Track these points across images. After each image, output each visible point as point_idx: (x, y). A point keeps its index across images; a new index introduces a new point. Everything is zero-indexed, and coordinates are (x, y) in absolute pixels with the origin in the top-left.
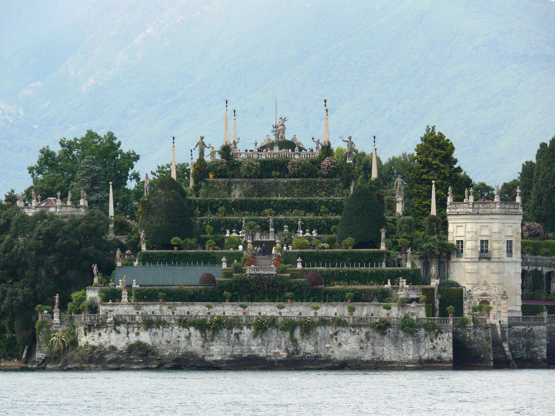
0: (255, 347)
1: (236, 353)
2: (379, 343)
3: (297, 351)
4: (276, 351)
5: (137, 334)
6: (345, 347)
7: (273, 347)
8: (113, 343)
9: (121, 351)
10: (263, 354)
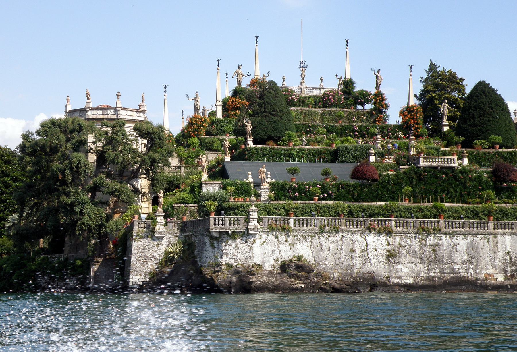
0: (459, 266)
1: (433, 274)
4: (490, 271)
5: (292, 245)
7: (484, 267)
8: (257, 260)
10: (471, 274)
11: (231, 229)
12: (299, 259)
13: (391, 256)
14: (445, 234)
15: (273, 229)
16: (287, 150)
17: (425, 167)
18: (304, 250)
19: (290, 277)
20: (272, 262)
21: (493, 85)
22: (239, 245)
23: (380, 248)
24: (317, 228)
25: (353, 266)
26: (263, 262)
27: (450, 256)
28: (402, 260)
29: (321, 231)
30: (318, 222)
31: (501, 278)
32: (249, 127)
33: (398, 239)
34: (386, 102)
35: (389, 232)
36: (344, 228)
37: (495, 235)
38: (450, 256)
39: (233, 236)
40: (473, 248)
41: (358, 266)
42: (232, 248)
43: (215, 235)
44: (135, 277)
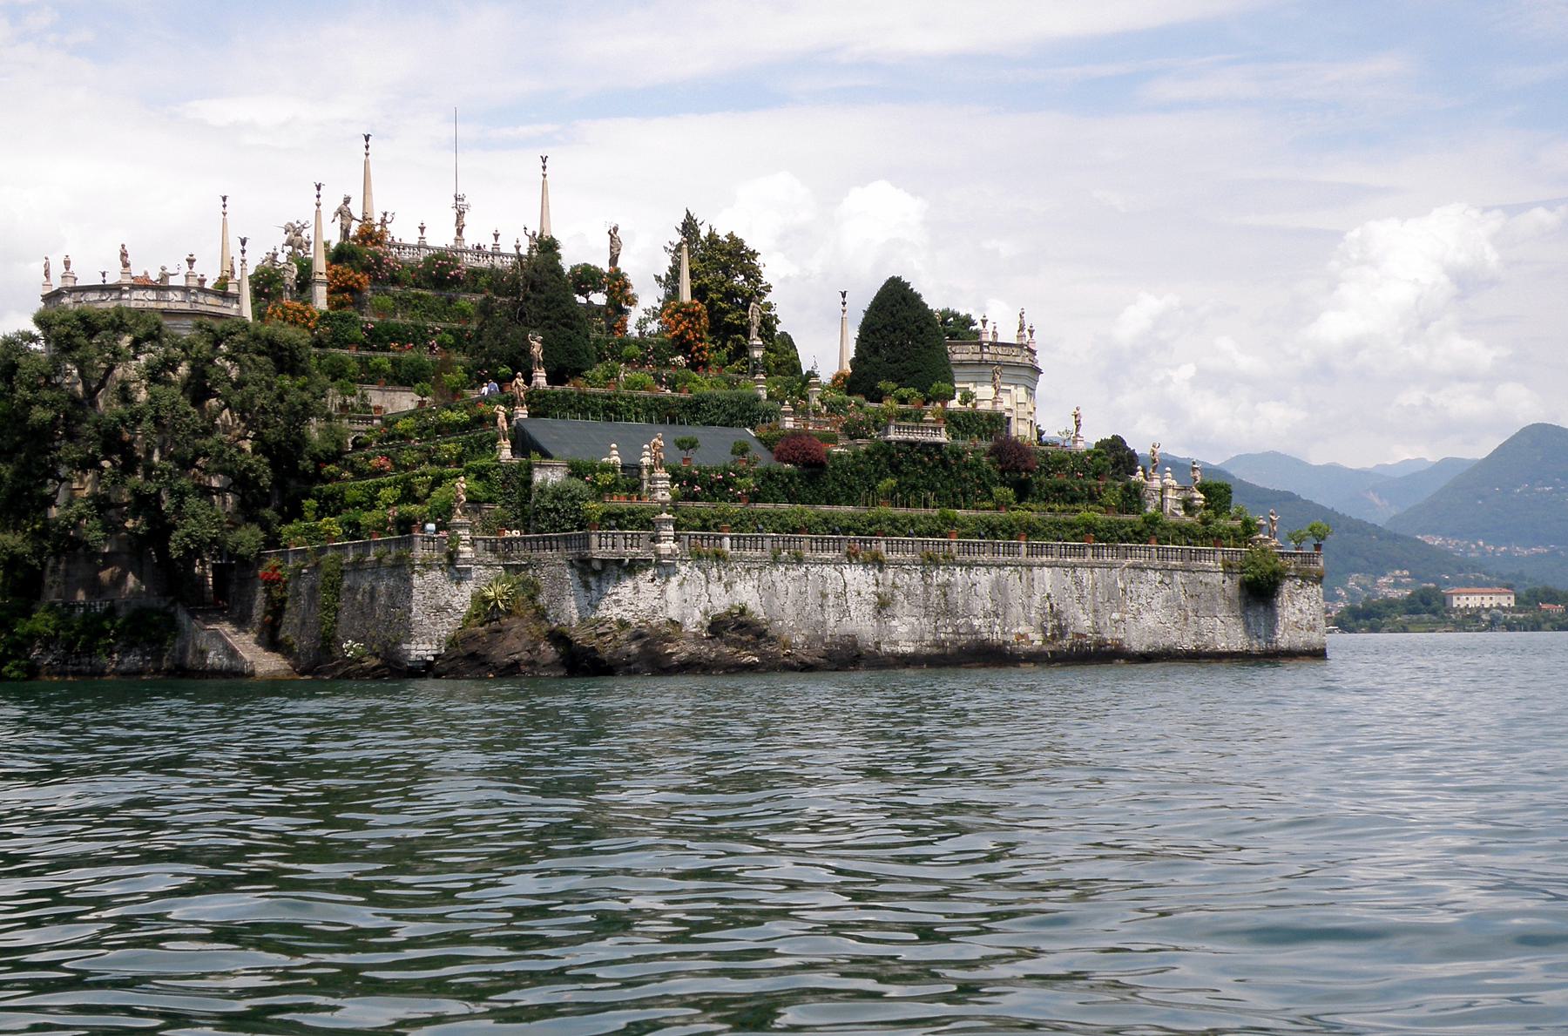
2: (1207, 609)
3: (1061, 631)
4: (1022, 630)
5: (729, 586)
6: (1149, 620)
8: (674, 613)
9: (695, 634)
10: (997, 636)
11: (629, 553)
12: (743, 611)
13: (883, 605)
14: (961, 565)
15: (700, 557)
16: (609, 398)
17: (898, 442)
18: (747, 593)
19: (727, 644)
20: (698, 616)
21: (916, 287)
22: (641, 583)
23: (864, 589)
24: (767, 553)
25: (824, 622)
26: (683, 616)
27: (967, 603)
28: (898, 611)
29: (776, 561)
30: (767, 543)
31: (1037, 640)
32: (536, 348)
33: (890, 572)
34: (631, 291)
35: (878, 562)
36: (808, 554)
37: (1030, 567)
38: (967, 603)
39: (631, 568)
40: (999, 588)
41: (834, 625)
42: (627, 591)
43: (597, 565)
44: (421, 646)
